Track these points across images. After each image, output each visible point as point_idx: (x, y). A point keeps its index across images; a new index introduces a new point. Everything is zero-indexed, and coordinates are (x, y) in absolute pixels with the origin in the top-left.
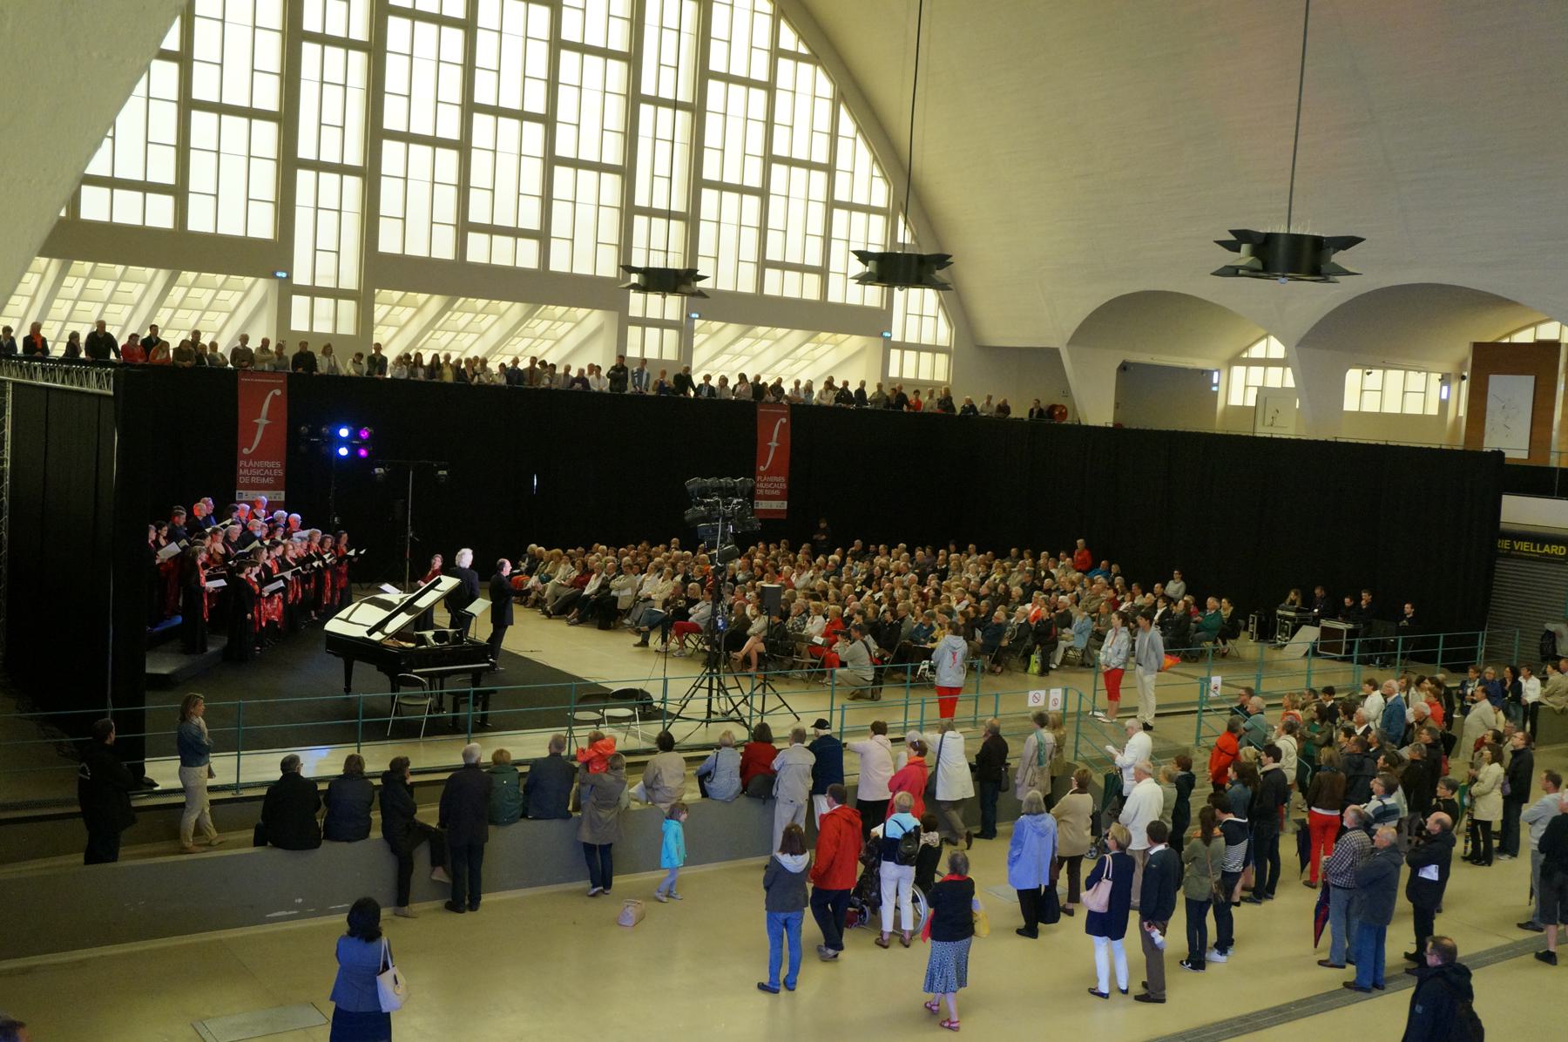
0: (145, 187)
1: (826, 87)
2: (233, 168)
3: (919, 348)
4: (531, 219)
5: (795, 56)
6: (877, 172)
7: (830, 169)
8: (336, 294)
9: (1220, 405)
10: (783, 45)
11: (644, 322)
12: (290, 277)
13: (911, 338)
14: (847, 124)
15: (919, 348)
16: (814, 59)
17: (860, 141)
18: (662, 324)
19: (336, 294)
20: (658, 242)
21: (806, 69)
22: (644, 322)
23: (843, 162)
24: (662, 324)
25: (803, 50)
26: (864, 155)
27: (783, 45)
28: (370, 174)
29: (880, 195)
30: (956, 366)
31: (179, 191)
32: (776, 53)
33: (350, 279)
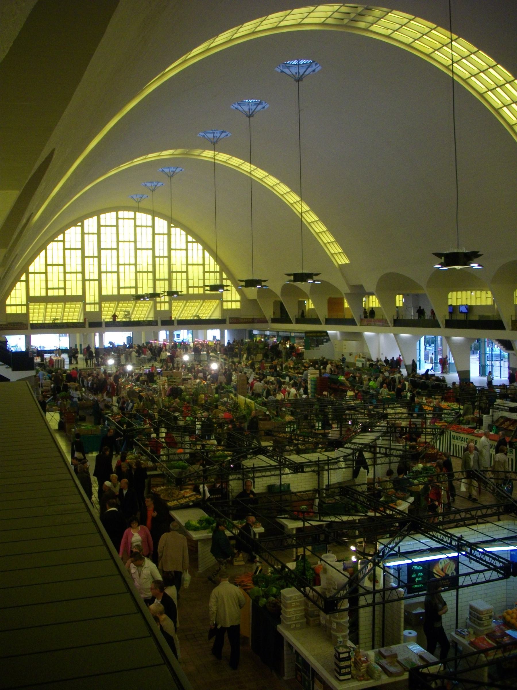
0: (59, 289)
1: (200, 247)
2: (74, 283)
3: (232, 301)
4: (133, 285)
5: (193, 242)
6: (216, 263)
7: (203, 265)
8: (94, 304)
9: (307, 308)
10: (189, 240)
11: (160, 302)
12: (85, 301)
13: (229, 299)
14: (207, 254)
15: (232, 301)
16: (197, 242)
17: (211, 257)
18: (165, 302)
19: (94, 304)
20: (162, 285)
21: (196, 244)
22: (160, 302)
23: (207, 262)
24: (165, 302)
25: (194, 240)
26: (212, 260)
27: (189, 240)
28: (99, 280)
29: (218, 268)
30: (242, 305)
31: (65, 288)
32: (187, 242)
33: (97, 301)
